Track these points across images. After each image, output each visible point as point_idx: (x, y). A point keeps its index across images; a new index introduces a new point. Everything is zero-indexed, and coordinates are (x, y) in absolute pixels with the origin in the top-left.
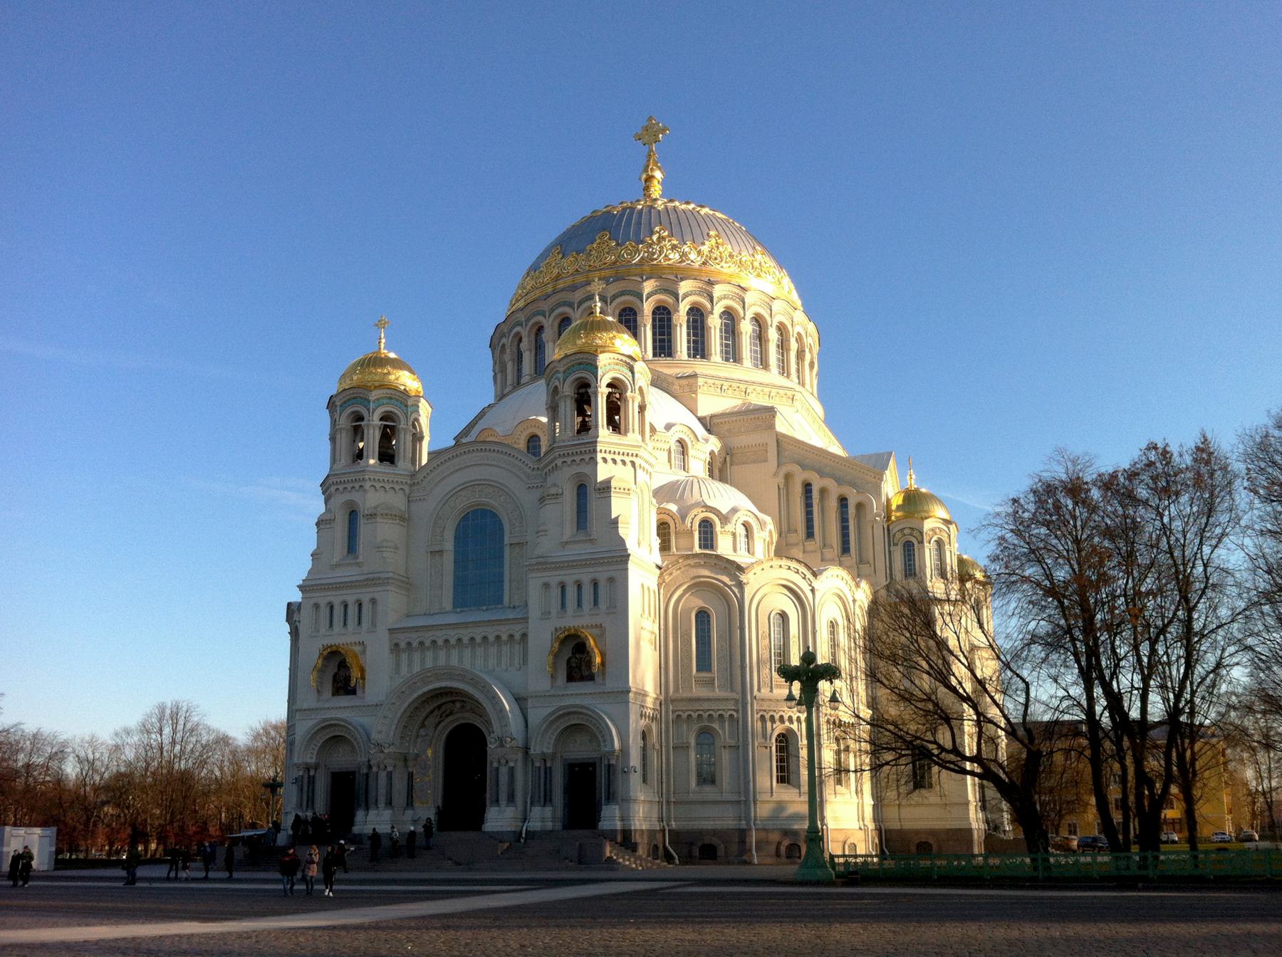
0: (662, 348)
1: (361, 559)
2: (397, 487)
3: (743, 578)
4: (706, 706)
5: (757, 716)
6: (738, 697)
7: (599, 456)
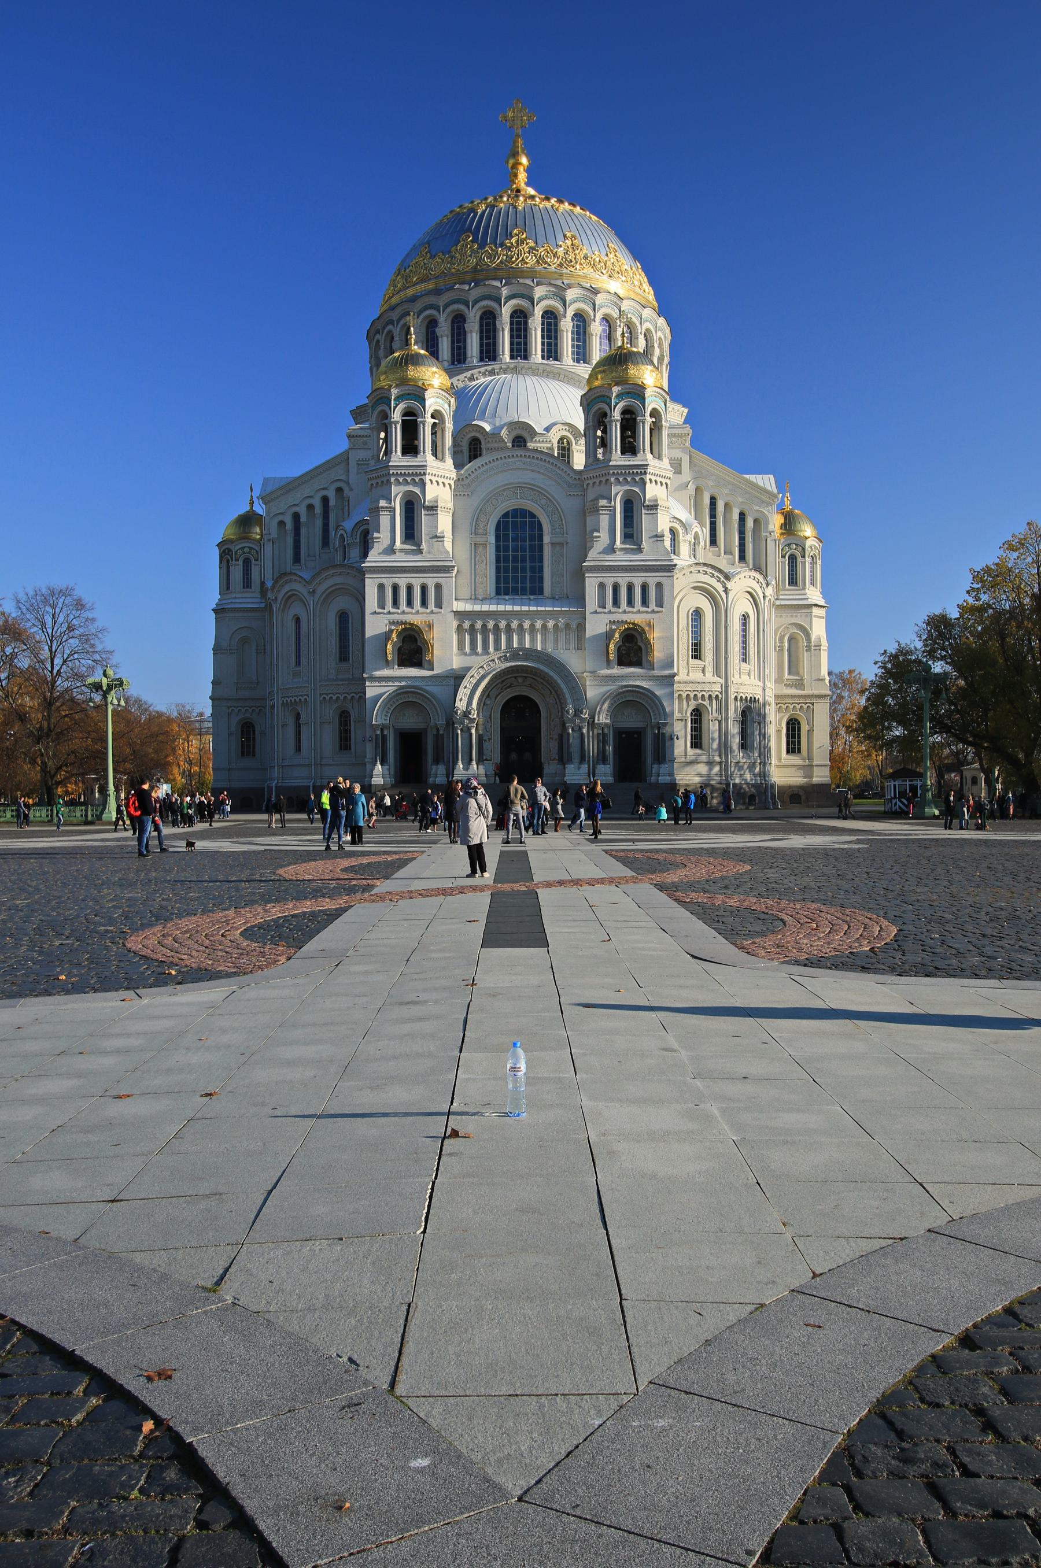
0: (578, 354)
1: (424, 546)
2: (447, 482)
3: (729, 585)
4: (700, 687)
5: (733, 697)
6: (722, 681)
7: (648, 477)
